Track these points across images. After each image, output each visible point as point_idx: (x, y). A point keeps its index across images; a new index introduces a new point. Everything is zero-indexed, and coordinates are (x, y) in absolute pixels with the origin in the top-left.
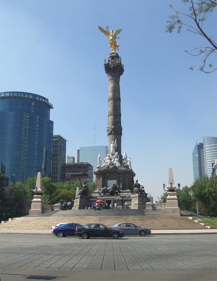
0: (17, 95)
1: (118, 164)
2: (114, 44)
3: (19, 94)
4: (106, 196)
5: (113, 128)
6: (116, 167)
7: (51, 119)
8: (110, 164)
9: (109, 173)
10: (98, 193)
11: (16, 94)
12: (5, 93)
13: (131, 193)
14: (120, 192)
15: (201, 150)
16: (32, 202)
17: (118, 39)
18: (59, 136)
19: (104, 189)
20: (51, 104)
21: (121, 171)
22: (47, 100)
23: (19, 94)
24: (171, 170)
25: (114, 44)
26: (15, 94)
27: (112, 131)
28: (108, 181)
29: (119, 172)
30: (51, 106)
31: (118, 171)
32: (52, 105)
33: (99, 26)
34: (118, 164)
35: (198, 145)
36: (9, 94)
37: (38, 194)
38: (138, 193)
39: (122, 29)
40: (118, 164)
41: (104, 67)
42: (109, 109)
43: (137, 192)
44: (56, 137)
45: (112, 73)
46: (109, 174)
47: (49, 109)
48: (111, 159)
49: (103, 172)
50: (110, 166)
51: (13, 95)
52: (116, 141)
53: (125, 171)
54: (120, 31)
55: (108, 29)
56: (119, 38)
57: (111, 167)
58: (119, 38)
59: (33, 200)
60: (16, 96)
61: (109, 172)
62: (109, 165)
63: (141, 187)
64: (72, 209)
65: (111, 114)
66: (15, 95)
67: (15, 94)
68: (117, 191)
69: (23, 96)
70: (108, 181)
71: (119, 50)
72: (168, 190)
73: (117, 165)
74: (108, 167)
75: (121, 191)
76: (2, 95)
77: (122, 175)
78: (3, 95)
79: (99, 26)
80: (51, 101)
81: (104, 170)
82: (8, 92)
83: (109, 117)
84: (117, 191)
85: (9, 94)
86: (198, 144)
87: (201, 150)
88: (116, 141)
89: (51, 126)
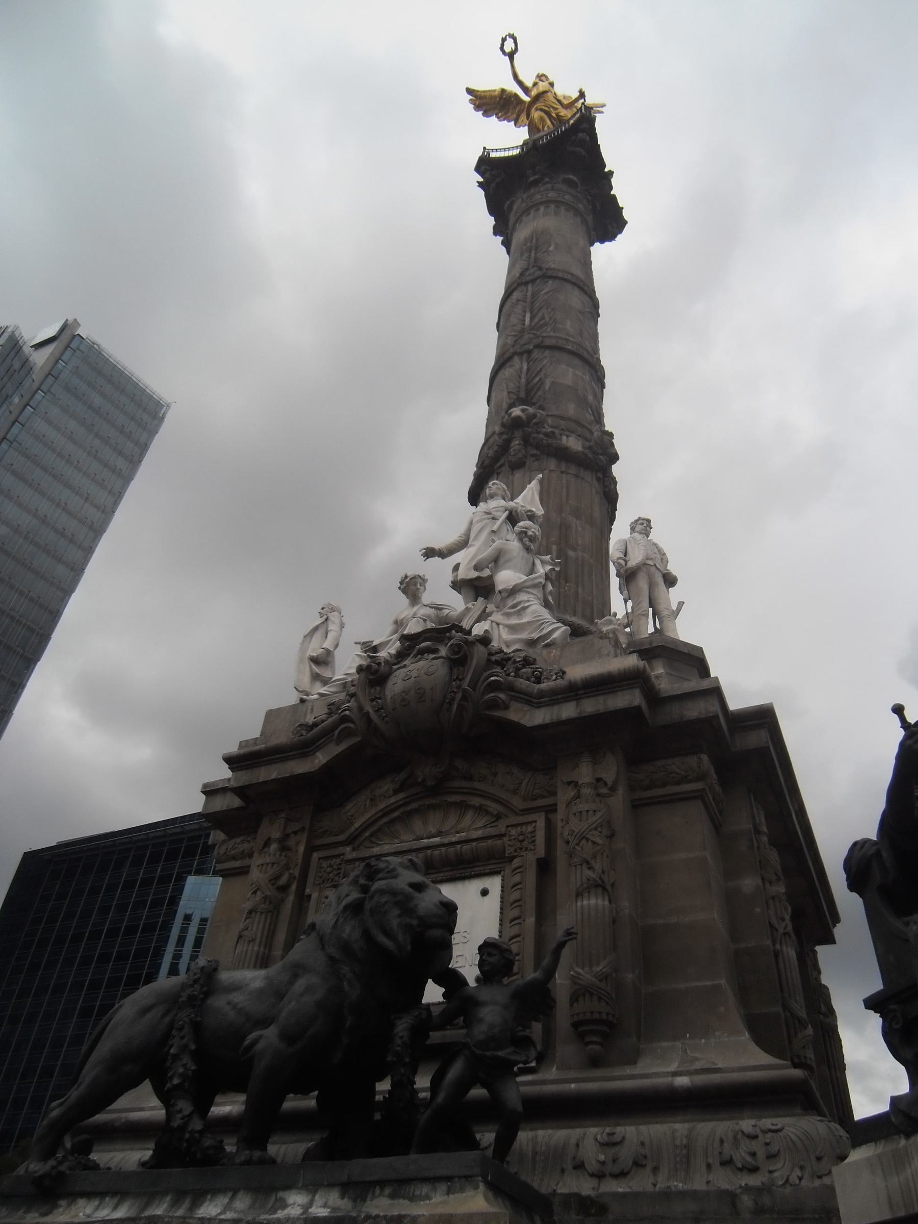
9: (386, 786)
21: (568, 711)
29: (539, 717)
33: (469, 91)
46: (387, 793)
77: (585, 773)
79: (469, 91)
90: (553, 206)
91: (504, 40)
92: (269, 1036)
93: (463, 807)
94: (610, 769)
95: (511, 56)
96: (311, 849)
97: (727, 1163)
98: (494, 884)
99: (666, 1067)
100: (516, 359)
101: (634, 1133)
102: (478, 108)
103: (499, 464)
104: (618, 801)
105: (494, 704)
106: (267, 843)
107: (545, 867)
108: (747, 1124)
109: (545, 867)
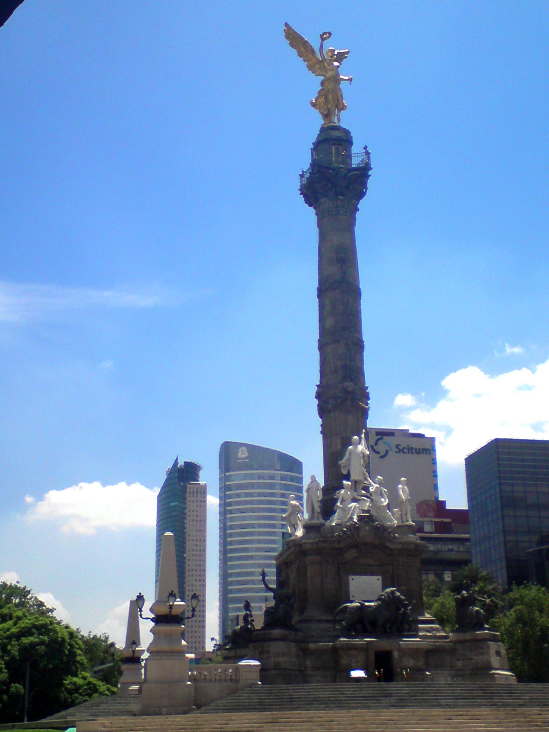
2: (330, 100)
5: (350, 389)
8: (360, 518)
9: (354, 551)
17: (349, 82)
21: (399, 546)
25: (330, 100)
31: (388, 544)
33: (286, 24)
35: (181, 470)
42: (329, 322)
45: (341, 197)
49: (336, 545)
52: (363, 436)
53: (412, 547)
55: (325, 42)
58: (350, 80)
61: (356, 546)
70: (351, 577)
79: (286, 24)
81: (339, 540)
83: (328, 349)
86: (181, 463)
88: (363, 436)
95: (323, 39)
98: (380, 577)
102: (287, 37)
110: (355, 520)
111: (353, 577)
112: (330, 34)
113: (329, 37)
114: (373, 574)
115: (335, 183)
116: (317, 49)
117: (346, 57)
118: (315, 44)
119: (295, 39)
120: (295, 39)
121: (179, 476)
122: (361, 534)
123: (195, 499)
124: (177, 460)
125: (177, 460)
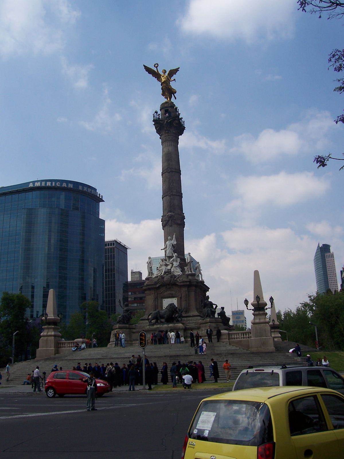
0: (52, 184)
1: (178, 272)
2: (168, 91)
3: (54, 183)
4: (159, 324)
6: (175, 276)
7: (101, 216)
8: (165, 272)
9: (164, 288)
10: (148, 319)
11: (50, 183)
12: (34, 182)
13: (199, 318)
14: (181, 316)
15: (326, 254)
16: (41, 337)
18: (116, 241)
19: (157, 313)
20: (99, 194)
22: (95, 190)
23: (54, 183)
24: (256, 273)
25: (168, 91)
26: (48, 183)
27: (169, 221)
28: (163, 300)
30: (101, 197)
32: (102, 196)
33: (144, 65)
34: (178, 272)
36: (39, 183)
37: (50, 323)
38: (210, 316)
39: (179, 68)
40: (179, 272)
41: (153, 123)
43: (208, 314)
44: (109, 244)
47: (97, 202)
48: (166, 265)
49: (155, 286)
50: (165, 275)
51: (46, 184)
52: (174, 236)
53: (188, 283)
54: (177, 70)
55: (158, 68)
56: (174, 80)
57: (166, 278)
58: (174, 80)
59: (42, 334)
60: (50, 185)
62: (164, 274)
63: (214, 306)
64: (108, 346)
65: (166, 194)
66: (48, 185)
67: (48, 183)
68: (177, 315)
69: (59, 185)
70: (163, 300)
71: (176, 98)
72: (253, 308)
73: (176, 274)
74: (162, 277)
75: (184, 315)
76: (30, 186)
77: (184, 289)
78: (32, 186)
79: (144, 65)
80: (100, 192)
81: (156, 283)
82: (37, 181)
84: (177, 315)
85: (39, 183)
87: (326, 254)
89: (102, 227)
90: (171, 141)
91: (155, 65)
92: (166, 316)
93: (172, 291)
94: (186, 289)
95: (157, 67)
96: (157, 294)
97: (194, 320)
98: (176, 299)
99: (191, 314)
100: (168, 197)
101: (188, 318)
103: (168, 224)
104: (187, 292)
105: (175, 282)
106: (152, 293)
107: (181, 298)
108: (195, 318)
109: (181, 298)
110: (162, 274)
111: (165, 299)
112: (158, 64)
113: (158, 65)
114: (172, 297)
115: (169, 125)
116: (157, 71)
117: (179, 70)
118: (155, 69)
119: (148, 70)
120: (148, 70)
121: (321, 251)
122: (165, 279)
123: (329, 259)
124: (319, 244)
125: (319, 244)
